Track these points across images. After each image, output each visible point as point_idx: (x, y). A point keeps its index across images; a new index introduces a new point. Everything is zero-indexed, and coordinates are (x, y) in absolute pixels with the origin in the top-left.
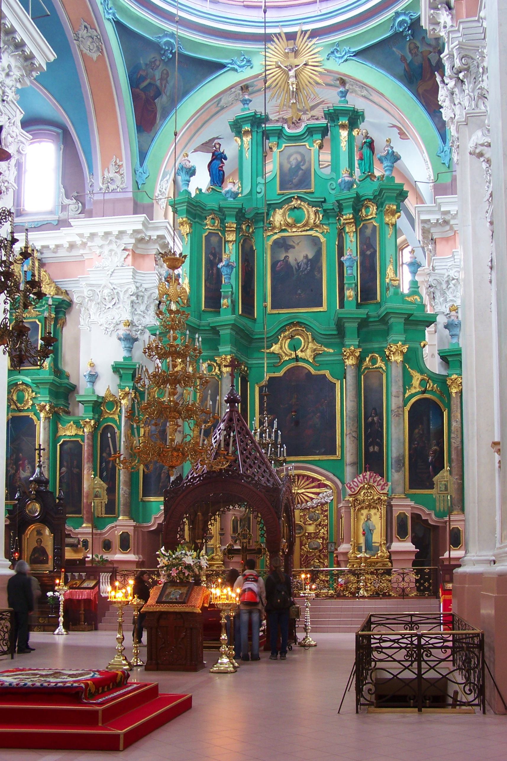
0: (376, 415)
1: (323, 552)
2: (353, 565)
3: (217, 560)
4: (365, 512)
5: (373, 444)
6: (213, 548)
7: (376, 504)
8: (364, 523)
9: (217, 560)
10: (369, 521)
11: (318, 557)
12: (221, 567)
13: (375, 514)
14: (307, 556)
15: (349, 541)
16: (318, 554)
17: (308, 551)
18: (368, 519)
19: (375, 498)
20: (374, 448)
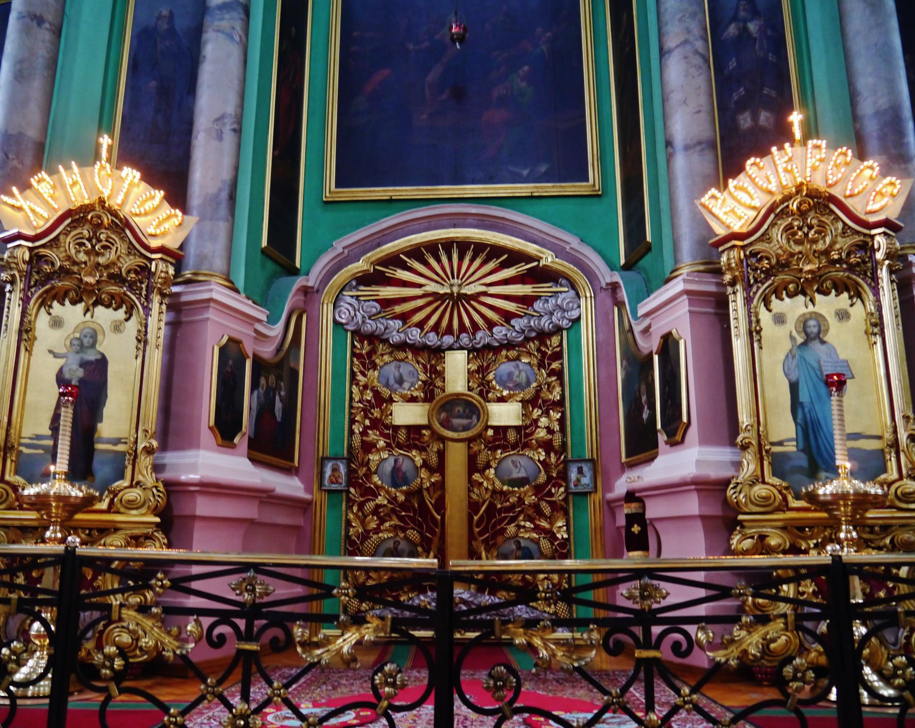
0: (755, 14)
1: (550, 494)
2: (762, 537)
3: (131, 505)
4: (794, 307)
5: (742, 106)
6: (123, 454)
7: (852, 268)
8: (790, 355)
9: (131, 505)
10: (816, 345)
11: (530, 512)
12: (148, 537)
13: (843, 315)
14: (492, 506)
15: (727, 429)
16: (530, 499)
17: (494, 492)
18: (812, 333)
19: (843, 243)
20: (755, 118)
